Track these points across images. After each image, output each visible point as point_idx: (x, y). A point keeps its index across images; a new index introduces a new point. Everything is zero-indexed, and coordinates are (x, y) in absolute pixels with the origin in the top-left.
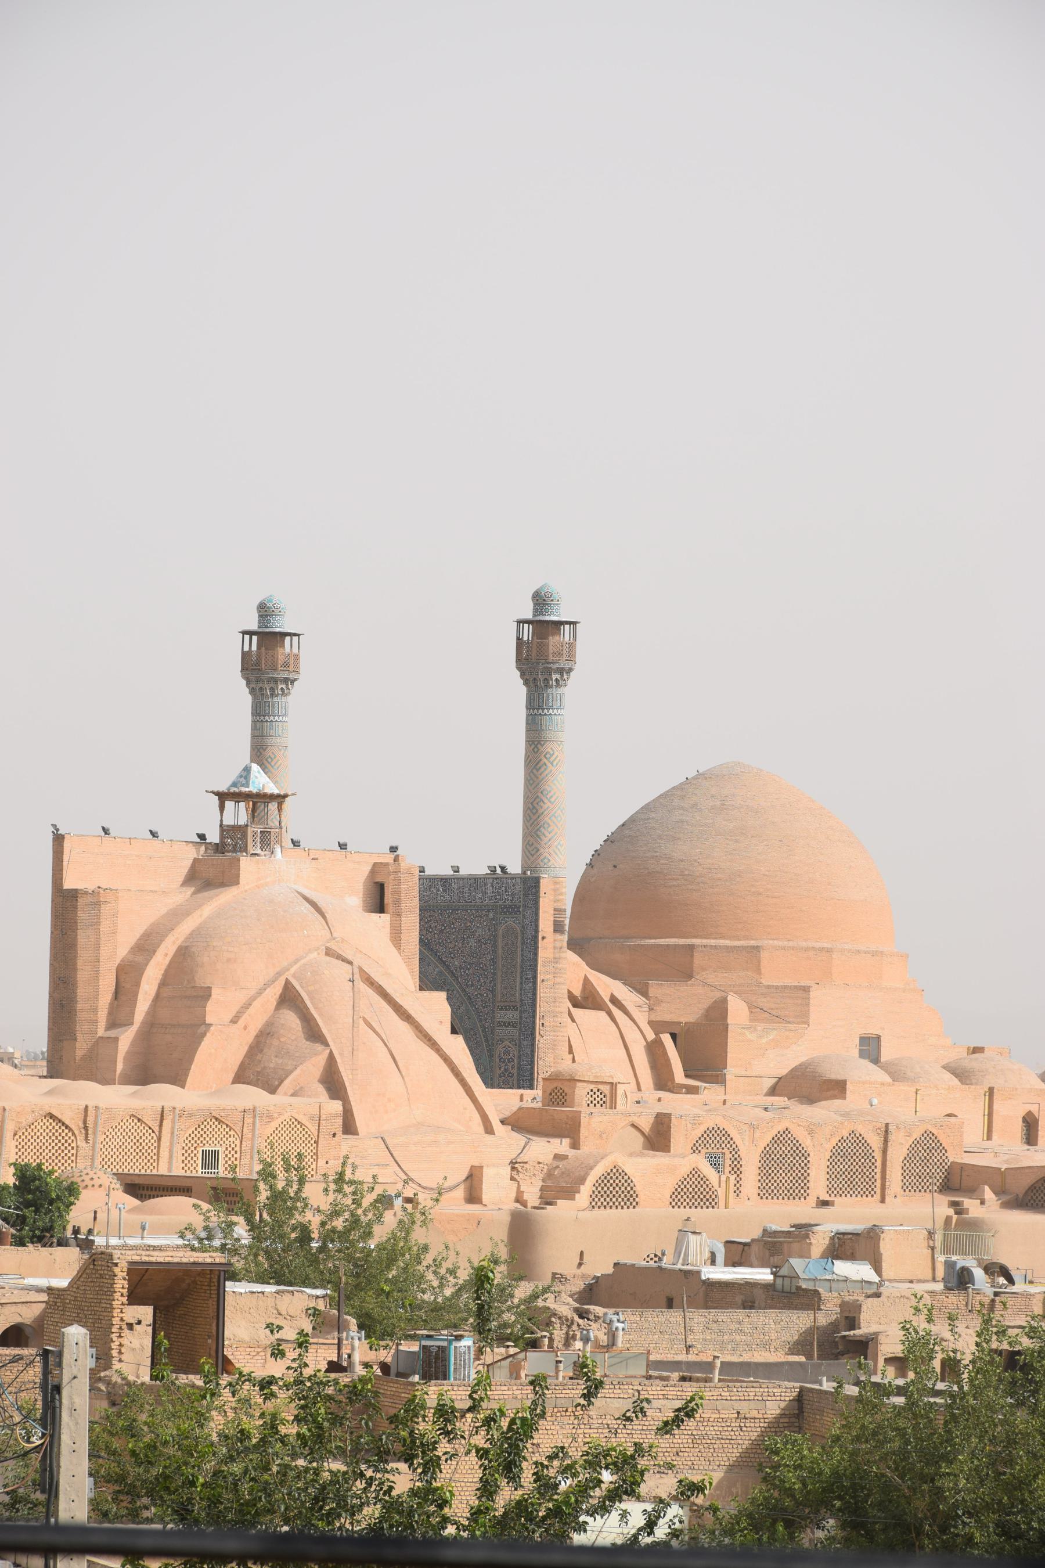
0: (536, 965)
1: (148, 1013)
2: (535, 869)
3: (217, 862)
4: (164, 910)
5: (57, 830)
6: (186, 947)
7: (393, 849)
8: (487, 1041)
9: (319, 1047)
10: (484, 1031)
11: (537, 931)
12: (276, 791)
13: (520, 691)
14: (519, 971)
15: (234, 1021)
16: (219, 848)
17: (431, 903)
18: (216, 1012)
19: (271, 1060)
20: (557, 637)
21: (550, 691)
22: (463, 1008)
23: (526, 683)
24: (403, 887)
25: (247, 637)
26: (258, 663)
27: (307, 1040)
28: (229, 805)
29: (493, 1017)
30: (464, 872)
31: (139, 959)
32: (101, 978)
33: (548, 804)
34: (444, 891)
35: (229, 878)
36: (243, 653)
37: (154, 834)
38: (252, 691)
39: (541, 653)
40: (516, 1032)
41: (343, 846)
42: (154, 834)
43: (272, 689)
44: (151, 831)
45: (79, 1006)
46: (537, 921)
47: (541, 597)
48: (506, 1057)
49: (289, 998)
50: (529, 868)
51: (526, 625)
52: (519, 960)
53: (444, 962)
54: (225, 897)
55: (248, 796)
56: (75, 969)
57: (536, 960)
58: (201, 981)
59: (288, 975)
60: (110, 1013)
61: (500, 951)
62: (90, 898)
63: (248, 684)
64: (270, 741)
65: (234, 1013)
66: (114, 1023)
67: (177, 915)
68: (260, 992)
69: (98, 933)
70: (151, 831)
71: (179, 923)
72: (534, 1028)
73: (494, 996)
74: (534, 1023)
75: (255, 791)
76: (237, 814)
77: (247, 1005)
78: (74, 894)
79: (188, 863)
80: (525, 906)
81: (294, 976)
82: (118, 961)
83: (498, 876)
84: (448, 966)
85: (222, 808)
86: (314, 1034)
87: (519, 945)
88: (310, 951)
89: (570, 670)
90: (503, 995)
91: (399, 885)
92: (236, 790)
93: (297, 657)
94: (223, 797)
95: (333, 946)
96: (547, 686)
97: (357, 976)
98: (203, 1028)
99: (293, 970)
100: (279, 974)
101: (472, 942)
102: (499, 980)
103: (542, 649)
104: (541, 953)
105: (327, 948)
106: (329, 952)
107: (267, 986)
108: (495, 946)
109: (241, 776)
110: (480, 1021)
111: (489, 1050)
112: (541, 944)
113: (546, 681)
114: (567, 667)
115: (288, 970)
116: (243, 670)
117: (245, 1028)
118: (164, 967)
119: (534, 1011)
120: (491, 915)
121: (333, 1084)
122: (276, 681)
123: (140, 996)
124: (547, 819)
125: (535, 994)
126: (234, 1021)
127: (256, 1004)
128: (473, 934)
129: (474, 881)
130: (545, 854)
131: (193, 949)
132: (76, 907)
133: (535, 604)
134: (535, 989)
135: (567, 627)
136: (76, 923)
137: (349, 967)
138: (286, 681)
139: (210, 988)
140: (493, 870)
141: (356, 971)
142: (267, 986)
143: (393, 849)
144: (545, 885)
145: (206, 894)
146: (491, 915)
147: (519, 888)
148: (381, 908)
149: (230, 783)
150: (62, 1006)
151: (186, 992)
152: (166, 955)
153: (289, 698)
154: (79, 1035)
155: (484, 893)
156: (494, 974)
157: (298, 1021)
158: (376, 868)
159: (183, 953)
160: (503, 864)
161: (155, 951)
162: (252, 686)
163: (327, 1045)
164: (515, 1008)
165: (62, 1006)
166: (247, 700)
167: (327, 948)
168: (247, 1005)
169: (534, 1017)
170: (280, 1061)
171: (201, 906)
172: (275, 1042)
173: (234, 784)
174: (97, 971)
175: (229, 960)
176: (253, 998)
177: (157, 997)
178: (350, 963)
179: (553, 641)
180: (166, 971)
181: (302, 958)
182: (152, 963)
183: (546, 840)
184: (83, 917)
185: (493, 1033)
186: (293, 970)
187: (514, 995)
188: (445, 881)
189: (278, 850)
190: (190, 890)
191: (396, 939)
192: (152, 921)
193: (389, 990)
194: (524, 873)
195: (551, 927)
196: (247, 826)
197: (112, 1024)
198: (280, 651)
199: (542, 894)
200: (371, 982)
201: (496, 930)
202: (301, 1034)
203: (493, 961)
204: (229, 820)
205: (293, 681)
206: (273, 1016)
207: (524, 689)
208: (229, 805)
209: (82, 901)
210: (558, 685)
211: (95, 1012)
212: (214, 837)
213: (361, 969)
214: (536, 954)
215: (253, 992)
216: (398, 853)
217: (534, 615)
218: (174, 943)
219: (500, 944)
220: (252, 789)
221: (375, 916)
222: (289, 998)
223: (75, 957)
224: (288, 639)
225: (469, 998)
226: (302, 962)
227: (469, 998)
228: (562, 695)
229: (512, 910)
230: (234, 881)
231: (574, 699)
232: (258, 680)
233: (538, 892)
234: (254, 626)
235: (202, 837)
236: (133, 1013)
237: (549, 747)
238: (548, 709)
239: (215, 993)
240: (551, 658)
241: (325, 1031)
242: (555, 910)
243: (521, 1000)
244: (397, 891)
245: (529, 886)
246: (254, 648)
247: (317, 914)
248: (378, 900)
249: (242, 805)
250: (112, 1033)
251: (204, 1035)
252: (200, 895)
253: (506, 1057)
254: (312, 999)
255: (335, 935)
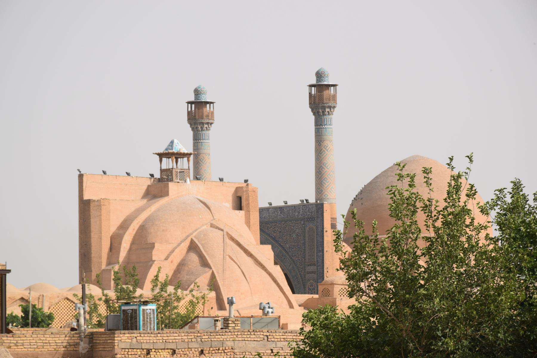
0: (323, 244)
1: (125, 257)
2: (321, 200)
3: (159, 187)
4: (133, 209)
5: (80, 172)
6: (143, 226)
7: (246, 181)
8: (302, 281)
9: (207, 269)
10: (301, 276)
11: (323, 228)
12: (186, 152)
13: (312, 118)
14: (316, 247)
15: (166, 259)
16: (160, 180)
17: (275, 219)
18: (158, 254)
19: (184, 277)
20: (327, 91)
21: (325, 117)
22: (291, 266)
23: (314, 114)
24: (250, 198)
25: (189, 105)
26: (195, 116)
27: (202, 266)
28: (164, 160)
29: (305, 270)
30: (289, 204)
31: (121, 232)
32: (103, 241)
33: (326, 169)
34: (281, 213)
35: (164, 193)
36: (188, 113)
37: (128, 174)
38: (193, 129)
39: (321, 99)
40: (315, 276)
41: (221, 180)
42: (128, 174)
43: (202, 128)
44: (127, 173)
45: (93, 255)
46: (323, 223)
47: (319, 74)
48: (311, 288)
49: (193, 247)
50: (319, 199)
51: (313, 88)
52: (316, 242)
53: (282, 246)
54: (162, 202)
55: (173, 154)
56: (90, 237)
57: (323, 242)
58: (150, 241)
59: (192, 237)
60: (109, 258)
61: (307, 239)
62: (96, 203)
63: (191, 126)
64: (201, 151)
65: (166, 255)
66: (110, 263)
67: (139, 211)
68: (179, 245)
69: (100, 220)
70: (127, 173)
71: (139, 214)
72: (323, 273)
73: (305, 260)
74: (323, 271)
75: (176, 152)
76: (167, 163)
77: (173, 251)
78: (89, 202)
79: (145, 187)
80: (317, 217)
81: (195, 237)
82: (111, 234)
83: (305, 205)
84: (284, 248)
85: (161, 161)
86: (205, 264)
87: (315, 235)
88: (203, 225)
89: (334, 107)
90: (309, 259)
91: (248, 196)
92: (167, 152)
93: (213, 113)
94: (161, 156)
95: (214, 222)
96: (324, 115)
97: (226, 236)
98: (151, 263)
99: (194, 234)
100: (188, 236)
101: (294, 236)
102: (307, 252)
103: (321, 98)
104: (325, 238)
105: (211, 224)
106: (212, 226)
107: (182, 242)
108: (304, 237)
109: (169, 146)
110: (299, 272)
111: (304, 285)
112: (325, 234)
113: (323, 112)
114: (332, 105)
115: (192, 234)
116: (189, 119)
117: (172, 262)
118: (133, 235)
119: (323, 266)
120: (302, 223)
121: (214, 285)
122: (203, 123)
123: (122, 249)
124: (326, 176)
125: (323, 258)
126: (166, 259)
127: (176, 250)
128: (294, 232)
129: (294, 207)
130: (326, 193)
131: (146, 226)
132: (89, 208)
133: (317, 77)
134: (323, 255)
135: (332, 88)
136: (90, 215)
137: (222, 232)
138: (208, 123)
139: (154, 243)
140: (302, 201)
141: (225, 234)
142: (182, 242)
143: (246, 181)
144: (326, 207)
145: (153, 201)
146: (302, 223)
147: (315, 209)
148: (240, 208)
149: (164, 149)
150: (85, 255)
151: (143, 245)
152: (134, 229)
153: (210, 132)
154: (93, 269)
155: (299, 213)
156: (305, 250)
157: (197, 258)
158: (237, 189)
159: (142, 228)
160: (307, 199)
161: (128, 228)
162: (193, 126)
163: (211, 268)
164: (314, 265)
165: (85, 255)
166: (191, 133)
167: (211, 224)
168: (173, 251)
169: (323, 268)
170: (188, 277)
171: (150, 206)
172: (186, 268)
173: (166, 149)
174: (101, 238)
175: (163, 230)
176: (175, 248)
177: (130, 250)
178: (222, 230)
179: (326, 93)
180: (134, 237)
181: (199, 228)
182: (127, 233)
183: (326, 186)
184: (93, 212)
185: (305, 277)
186: (194, 234)
187: (314, 259)
188: (281, 208)
189: (188, 180)
190: (145, 201)
191: (248, 223)
192: (128, 214)
193: (242, 242)
194: (316, 202)
195: (330, 226)
196: (172, 168)
197: (109, 263)
198: (205, 110)
199: (325, 211)
200: (232, 239)
201: (305, 229)
202: (198, 264)
203: (304, 244)
204: (164, 167)
205: (211, 124)
206: (185, 256)
207: (313, 117)
208: (164, 160)
209: (92, 205)
210: (329, 114)
211: (100, 257)
212: (157, 175)
213: (227, 233)
214: (323, 239)
215: (175, 245)
216: (248, 182)
217: (318, 81)
218: (138, 223)
219: (307, 235)
220: (175, 151)
221: (237, 212)
222: (193, 247)
223: (90, 232)
224: (208, 105)
225: (294, 261)
226: (199, 230)
227: (294, 261)
228: (331, 119)
229: (311, 219)
230: (166, 194)
231: (337, 120)
232: (195, 124)
233: (323, 210)
234: (192, 99)
235: (152, 175)
236: (118, 258)
237: (325, 143)
238: (325, 125)
239: (157, 245)
240: (325, 101)
241: (210, 262)
242: (331, 218)
243: (317, 261)
244: (247, 200)
245: (319, 208)
246: (193, 109)
247: (206, 208)
248: (239, 203)
249: (170, 159)
250: (110, 267)
251: (151, 266)
252: (150, 202)
253: (311, 288)
254: (203, 247)
255: (215, 217)
